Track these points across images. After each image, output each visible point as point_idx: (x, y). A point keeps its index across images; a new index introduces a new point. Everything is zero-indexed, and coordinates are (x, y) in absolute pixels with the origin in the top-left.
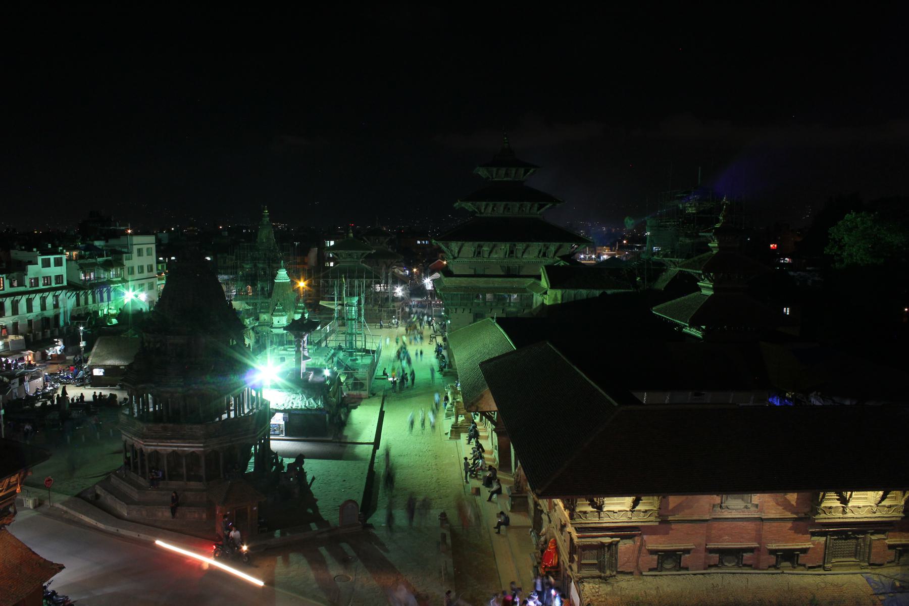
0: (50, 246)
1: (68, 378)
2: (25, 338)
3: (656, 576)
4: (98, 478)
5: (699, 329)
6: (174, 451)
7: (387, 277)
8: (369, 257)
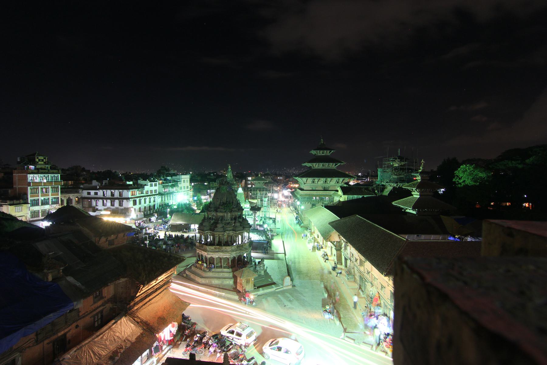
0: (152, 179)
2: (144, 213)
5: (416, 211)
6: (219, 257)
8: (266, 183)
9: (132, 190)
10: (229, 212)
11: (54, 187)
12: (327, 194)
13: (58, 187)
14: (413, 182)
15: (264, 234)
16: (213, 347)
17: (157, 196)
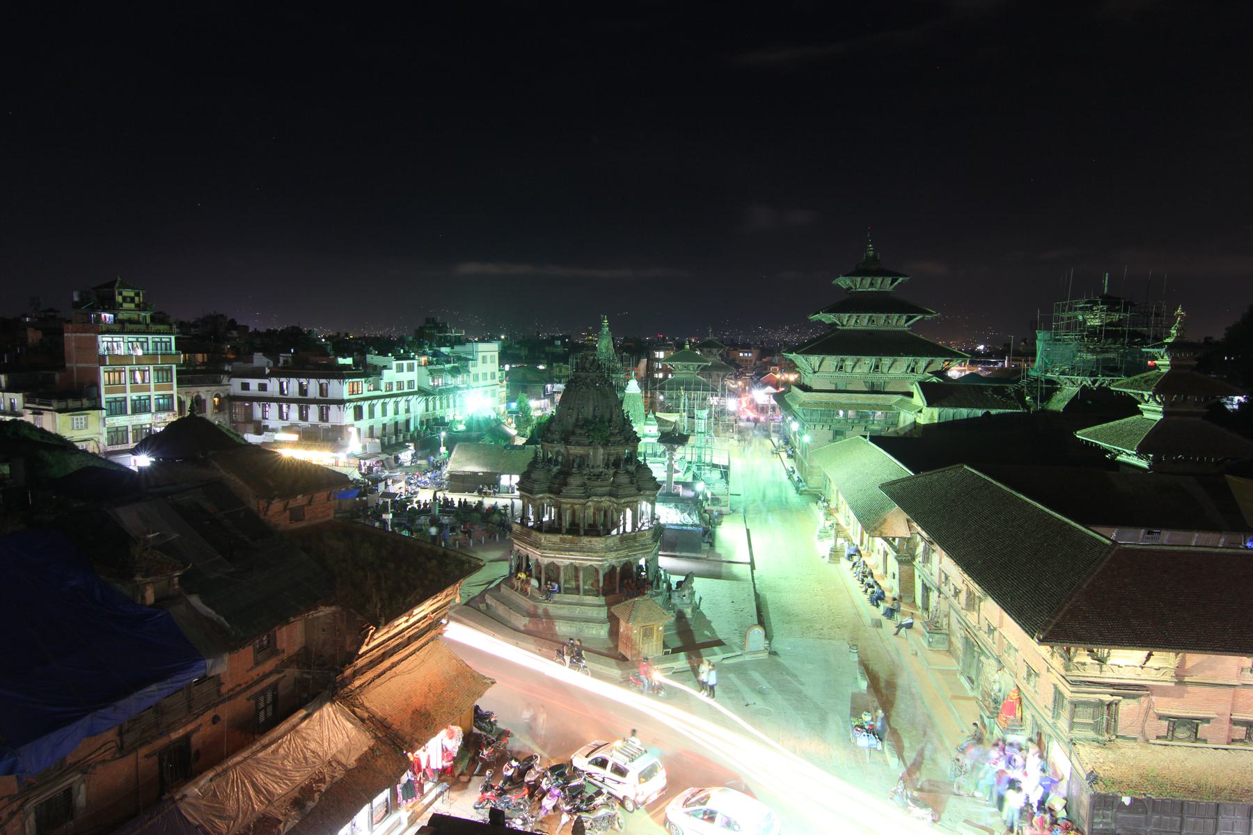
0: (402, 351)
2: (381, 442)
3: (1166, 745)
6: (571, 564)
8: (705, 369)
9: (350, 380)
10: (599, 446)
11: (162, 369)
12: (880, 402)
13: (171, 367)
14: (1145, 375)
15: (694, 508)
16: (553, 796)
17: (416, 396)
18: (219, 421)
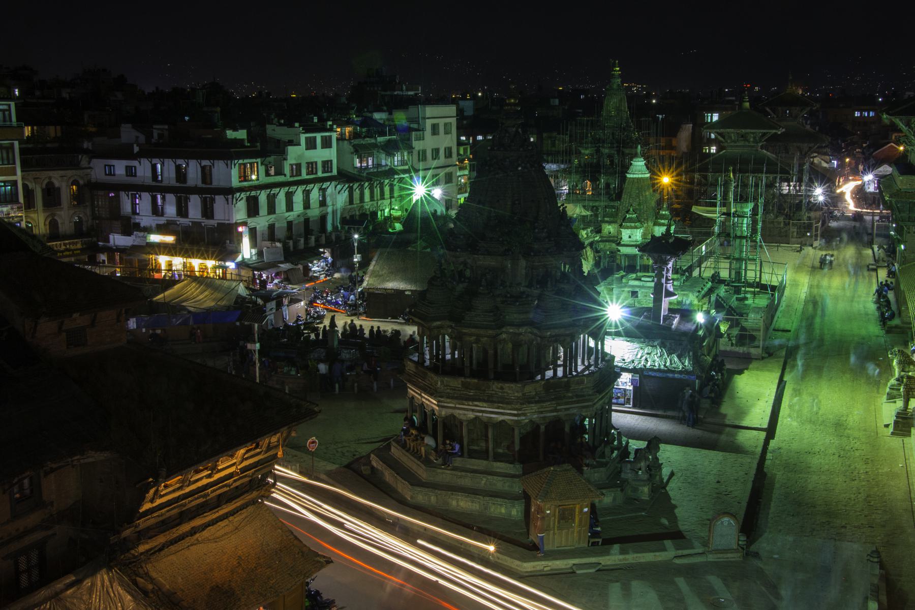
0: (316, 120)
1: (337, 303)
4: (377, 444)
6: (477, 418)
7: (801, 171)
8: (775, 138)
9: (241, 161)
13: (12, 145)
15: (689, 346)
17: (333, 183)
18: (79, 217)
